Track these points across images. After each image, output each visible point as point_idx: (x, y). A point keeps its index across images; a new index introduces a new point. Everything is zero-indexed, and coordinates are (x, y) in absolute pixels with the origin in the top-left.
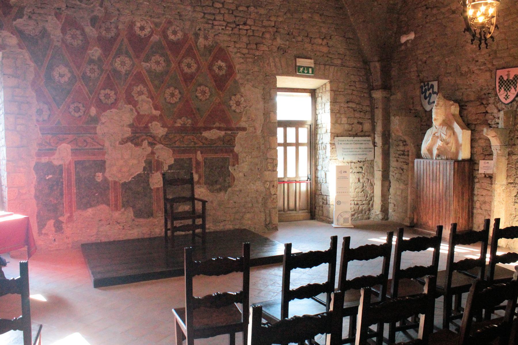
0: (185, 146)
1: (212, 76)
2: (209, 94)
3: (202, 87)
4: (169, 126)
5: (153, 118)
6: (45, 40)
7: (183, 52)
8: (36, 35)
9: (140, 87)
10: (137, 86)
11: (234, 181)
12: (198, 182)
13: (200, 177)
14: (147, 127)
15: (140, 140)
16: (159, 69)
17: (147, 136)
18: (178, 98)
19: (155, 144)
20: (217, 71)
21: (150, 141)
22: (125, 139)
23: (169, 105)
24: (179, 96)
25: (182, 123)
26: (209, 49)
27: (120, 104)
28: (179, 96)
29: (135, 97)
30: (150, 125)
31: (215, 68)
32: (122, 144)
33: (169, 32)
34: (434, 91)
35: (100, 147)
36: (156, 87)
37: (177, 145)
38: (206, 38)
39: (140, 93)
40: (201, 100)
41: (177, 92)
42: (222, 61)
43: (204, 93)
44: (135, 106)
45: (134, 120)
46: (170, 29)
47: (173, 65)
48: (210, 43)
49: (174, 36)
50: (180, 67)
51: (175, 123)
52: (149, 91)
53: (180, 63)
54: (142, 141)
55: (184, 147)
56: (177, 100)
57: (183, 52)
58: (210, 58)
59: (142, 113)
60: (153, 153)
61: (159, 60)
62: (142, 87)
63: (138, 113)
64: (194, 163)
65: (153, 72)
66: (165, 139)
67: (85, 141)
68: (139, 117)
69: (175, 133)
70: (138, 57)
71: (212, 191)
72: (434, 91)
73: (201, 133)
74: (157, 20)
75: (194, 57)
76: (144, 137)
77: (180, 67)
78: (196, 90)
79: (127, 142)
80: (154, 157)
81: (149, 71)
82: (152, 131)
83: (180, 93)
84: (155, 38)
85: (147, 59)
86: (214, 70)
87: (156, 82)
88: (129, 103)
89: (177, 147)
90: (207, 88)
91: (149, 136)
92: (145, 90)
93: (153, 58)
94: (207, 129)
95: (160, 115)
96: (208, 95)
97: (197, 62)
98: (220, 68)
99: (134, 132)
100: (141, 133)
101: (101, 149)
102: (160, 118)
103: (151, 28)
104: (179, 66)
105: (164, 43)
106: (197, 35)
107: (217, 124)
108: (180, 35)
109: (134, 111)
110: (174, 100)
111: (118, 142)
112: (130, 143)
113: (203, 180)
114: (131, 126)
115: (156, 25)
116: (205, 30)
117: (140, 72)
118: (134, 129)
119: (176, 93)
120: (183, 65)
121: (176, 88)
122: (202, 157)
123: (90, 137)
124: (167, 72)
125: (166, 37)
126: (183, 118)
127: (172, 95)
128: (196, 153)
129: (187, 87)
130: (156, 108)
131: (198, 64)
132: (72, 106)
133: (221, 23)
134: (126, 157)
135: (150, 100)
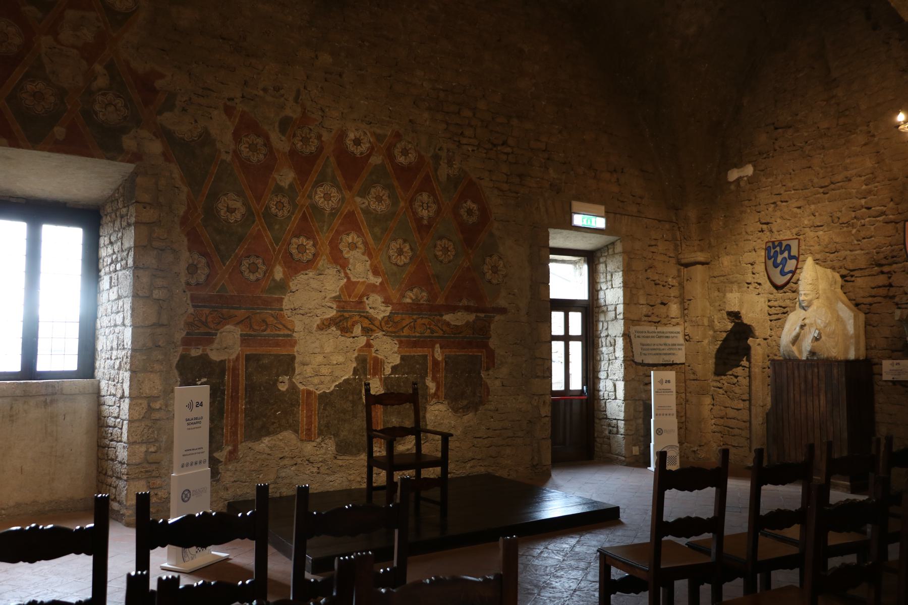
0: (418, 335)
4: (395, 301)
5: (372, 288)
9: (351, 238)
10: (348, 235)
11: (488, 394)
12: (435, 395)
13: (438, 389)
14: (361, 302)
15: (349, 324)
16: (381, 208)
17: (361, 316)
19: (372, 330)
21: (364, 325)
22: (327, 319)
27: (320, 263)
29: (344, 252)
32: (322, 329)
34: (792, 254)
35: (287, 332)
36: (375, 237)
39: (353, 246)
45: (341, 290)
52: (365, 243)
54: (353, 325)
59: (353, 279)
60: (368, 345)
63: (349, 279)
64: (430, 364)
66: (387, 323)
67: (264, 321)
68: (350, 286)
70: (350, 188)
71: (455, 411)
72: (792, 254)
74: (379, 131)
76: (357, 318)
79: (329, 326)
80: (370, 352)
81: (366, 212)
84: (376, 160)
85: (364, 193)
87: (377, 230)
92: (359, 241)
93: (373, 190)
94: (453, 309)
99: (341, 309)
101: (288, 336)
102: (381, 289)
103: (370, 142)
109: (343, 275)
111: (315, 326)
112: (334, 328)
113: (442, 393)
114: (337, 299)
115: (379, 138)
118: (342, 304)
122: (442, 353)
123: (272, 315)
128: (433, 347)
130: (376, 272)
134: (328, 349)
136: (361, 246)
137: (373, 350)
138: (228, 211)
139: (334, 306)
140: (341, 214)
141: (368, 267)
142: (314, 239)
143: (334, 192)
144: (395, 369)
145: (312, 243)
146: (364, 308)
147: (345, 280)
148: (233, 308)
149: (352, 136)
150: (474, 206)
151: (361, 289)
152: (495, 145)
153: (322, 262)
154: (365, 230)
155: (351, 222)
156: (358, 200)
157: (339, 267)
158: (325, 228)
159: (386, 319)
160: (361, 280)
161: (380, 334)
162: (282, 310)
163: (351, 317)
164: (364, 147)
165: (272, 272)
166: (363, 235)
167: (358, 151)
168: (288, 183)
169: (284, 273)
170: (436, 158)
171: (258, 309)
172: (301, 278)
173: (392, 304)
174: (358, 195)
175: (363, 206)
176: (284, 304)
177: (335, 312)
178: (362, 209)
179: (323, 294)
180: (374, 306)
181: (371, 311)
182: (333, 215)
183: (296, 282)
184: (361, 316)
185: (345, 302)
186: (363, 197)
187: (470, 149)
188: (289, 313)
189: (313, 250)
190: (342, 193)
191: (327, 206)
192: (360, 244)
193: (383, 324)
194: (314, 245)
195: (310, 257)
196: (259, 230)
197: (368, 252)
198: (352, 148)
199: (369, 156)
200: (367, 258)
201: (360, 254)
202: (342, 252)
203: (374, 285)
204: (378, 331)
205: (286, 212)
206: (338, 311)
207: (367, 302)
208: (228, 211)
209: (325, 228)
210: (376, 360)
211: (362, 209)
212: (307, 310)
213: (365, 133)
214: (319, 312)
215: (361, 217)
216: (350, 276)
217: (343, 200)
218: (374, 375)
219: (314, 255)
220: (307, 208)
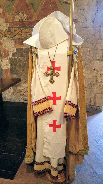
25: (20, 18)
37: (17, 38)
51: (14, 18)
55: (22, 39)
66: (8, 33)
69: (15, 28)
89: (18, 39)
95: (3, 12)
126: (20, 14)
137: (3, 46)
144: (14, 54)
159: (7, 31)
161: (6, 38)
173: (9, 22)
193: (6, 33)
204: (4, 37)
210: (5, 51)
218: (5, 57)
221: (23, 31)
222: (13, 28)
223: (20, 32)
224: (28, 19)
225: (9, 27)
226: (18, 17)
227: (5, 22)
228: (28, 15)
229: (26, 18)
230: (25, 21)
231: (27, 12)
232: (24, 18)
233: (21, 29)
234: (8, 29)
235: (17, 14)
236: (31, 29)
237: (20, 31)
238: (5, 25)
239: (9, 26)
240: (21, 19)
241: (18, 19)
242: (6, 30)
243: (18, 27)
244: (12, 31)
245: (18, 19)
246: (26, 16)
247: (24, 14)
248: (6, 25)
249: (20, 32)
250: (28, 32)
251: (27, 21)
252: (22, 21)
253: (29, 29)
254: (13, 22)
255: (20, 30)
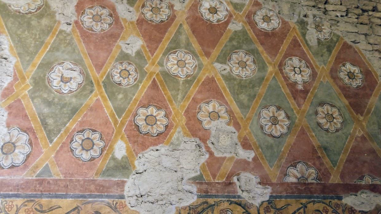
1: (340, 87)
2: (341, 120)
3: (325, 107)
5: (243, 165)
6: (45, 21)
7: (284, 47)
8: (30, 13)
9: (213, 106)
10: (208, 103)
17: (231, 203)
18: (285, 127)
20: (346, 80)
22: (184, 208)
23: (270, 139)
24: (287, 122)
25: (299, 175)
26: (327, 46)
27: (175, 136)
28: (287, 122)
29: (204, 123)
30: (235, 179)
31: (342, 75)
33: (258, 18)
36: (242, 106)
38: (318, 27)
40: (327, 130)
41: (281, 116)
42: (354, 65)
43: (330, 117)
44: (204, 140)
45: (203, 168)
46: (259, 13)
47: (270, 69)
48: (327, 36)
49: (265, 23)
50: (282, 73)
52: (230, 113)
53: (281, 66)
56: (285, 131)
57: (284, 47)
58: (331, 59)
59: (217, 154)
61: (245, 60)
62: (217, 105)
63: (211, 154)
65: (235, 79)
68: (214, 163)
69: (286, 197)
70: (208, 54)
73: (340, 198)
75: (303, 57)
76: (226, 205)
77: (282, 73)
78: (316, 113)
81: (229, 78)
82: (240, 193)
83: (288, 117)
84: (235, 26)
85: (224, 58)
86: (341, 79)
87: (243, 97)
88: (194, 135)
90: (334, 109)
91: (236, 203)
93: (234, 56)
95: (255, 159)
96: (338, 121)
97: (309, 65)
98: (351, 75)
99: (204, 194)
100: (216, 196)
102: (255, 165)
103: (227, 10)
104: (281, 70)
105: (251, 34)
106: (303, 24)
107: (368, 180)
108: (275, 23)
109: (204, 150)
110: (278, 130)
114: (198, 180)
116: (314, 16)
117: (213, 78)
118: (204, 187)
119: (280, 118)
120: (287, 69)
121: (279, 108)
124: (262, 79)
125: (252, 24)
126: (299, 166)
127: (272, 121)
129: (299, 106)
130: (246, 145)
131: (313, 68)
132: (78, 138)
133: (339, 7)
135: (232, 128)
136: (225, 115)
138: (62, 81)
139: (194, 189)
140: (198, 81)
141: (236, 140)
142: (166, 108)
143: (189, 58)
145: (163, 113)
146: (235, 192)
147: (207, 156)
148: (57, 197)
149: (206, 5)
150: (355, 69)
151: (228, 167)
152: (364, 11)
153: (177, 134)
154: (229, 97)
155: (211, 89)
156: (218, 66)
157: (197, 140)
158: (180, 97)
159: (265, 205)
160: (228, 155)
162: (122, 197)
163: (217, 204)
164: (221, 15)
165: (111, 148)
166: (227, 103)
167: (214, 19)
168: (135, 50)
169: (128, 150)
170: (303, 24)
171: (90, 196)
172: (150, 154)
173: (271, 184)
174: (218, 61)
175: (224, 73)
176: (126, 188)
177: (196, 197)
178: (223, 75)
179: (179, 174)
180: (248, 188)
181: (244, 195)
182: (190, 80)
183: (143, 160)
184: (231, 203)
185: (209, 184)
186: (224, 63)
187: (339, 15)
188: (133, 201)
189: (165, 121)
190: (198, 60)
191: (182, 74)
192: (223, 113)
194: (166, 116)
195: (162, 129)
196: (98, 100)
197: (234, 121)
198: (207, 16)
199: (227, 23)
200: (233, 129)
201: (224, 125)
202: (201, 122)
203: (246, 162)
205: (132, 80)
206: (199, 197)
207: (238, 184)
208: (62, 81)
209: (180, 97)
211: (223, 75)
212: (157, 197)
213: (221, 3)
214: (174, 198)
215: (222, 84)
216: (213, 150)
217: (200, 66)
219: (167, 127)
220: (158, 75)
221: (309, 206)
222: (281, 197)
223: (302, 210)
224: (317, 178)
225: (271, 197)
226: (295, 172)
227: (260, 183)
228: (318, 170)
229: (314, 175)
230: (312, 184)
231: (314, 164)
232: (310, 175)
233: (304, 201)
234: (268, 201)
235: (291, 166)
236: (328, 203)
237: (301, 206)
238: (259, 189)
239: (271, 193)
240: (303, 177)
241: (296, 177)
242: (263, 202)
243: (295, 197)
244: (279, 207)
245: (296, 177)
246: (313, 171)
247: (309, 167)
248: (262, 190)
249: (302, 210)
250: (321, 209)
251: (317, 184)
252: (305, 184)
253: (323, 203)
254: (282, 184)
255: (301, 204)
